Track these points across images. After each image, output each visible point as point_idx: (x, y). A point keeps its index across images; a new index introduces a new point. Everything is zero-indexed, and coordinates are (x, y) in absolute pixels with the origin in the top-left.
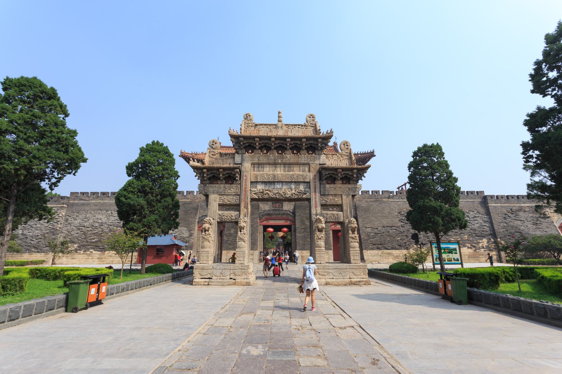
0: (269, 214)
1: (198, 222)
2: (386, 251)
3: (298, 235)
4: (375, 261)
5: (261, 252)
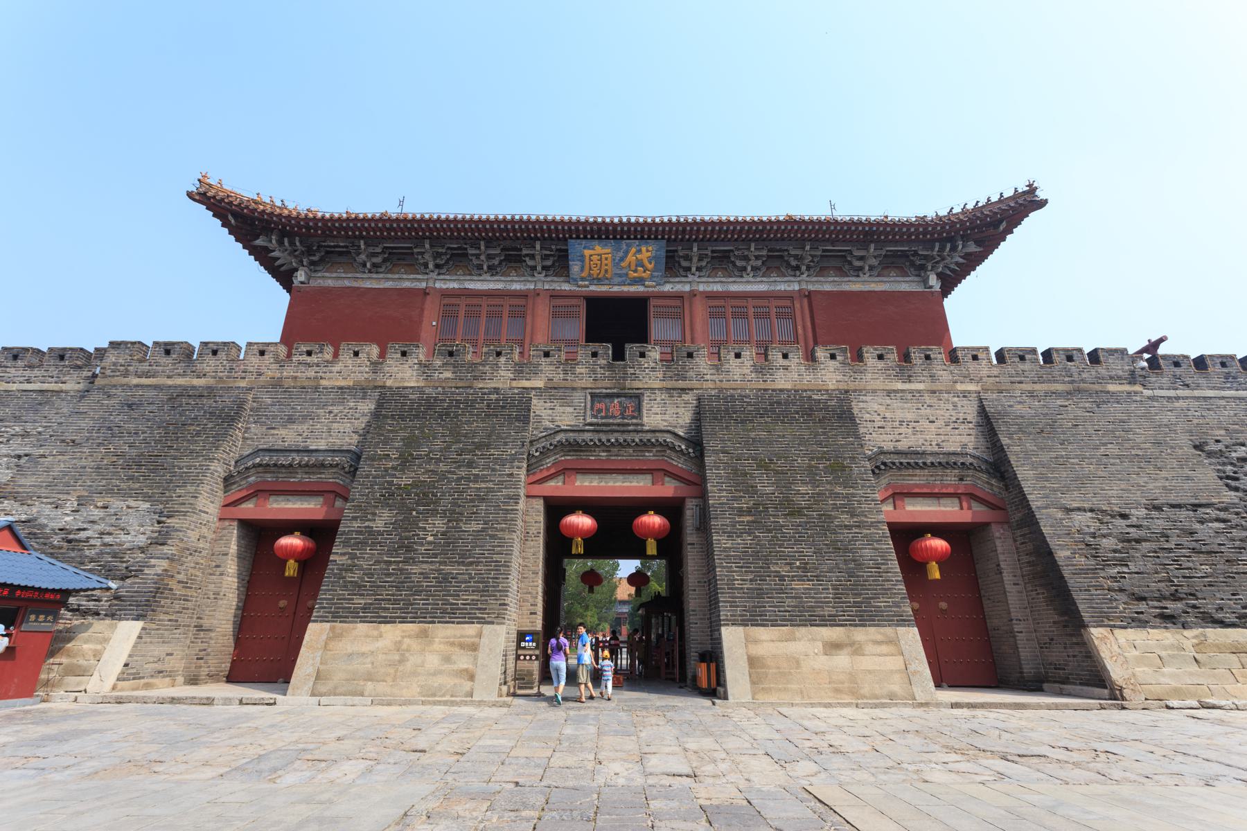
0: (573, 447)
1: (228, 481)
2: (1215, 634)
3: (721, 541)
4: (1178, 693)
5: (521, 636)
